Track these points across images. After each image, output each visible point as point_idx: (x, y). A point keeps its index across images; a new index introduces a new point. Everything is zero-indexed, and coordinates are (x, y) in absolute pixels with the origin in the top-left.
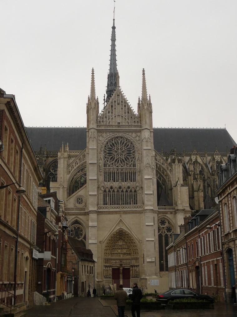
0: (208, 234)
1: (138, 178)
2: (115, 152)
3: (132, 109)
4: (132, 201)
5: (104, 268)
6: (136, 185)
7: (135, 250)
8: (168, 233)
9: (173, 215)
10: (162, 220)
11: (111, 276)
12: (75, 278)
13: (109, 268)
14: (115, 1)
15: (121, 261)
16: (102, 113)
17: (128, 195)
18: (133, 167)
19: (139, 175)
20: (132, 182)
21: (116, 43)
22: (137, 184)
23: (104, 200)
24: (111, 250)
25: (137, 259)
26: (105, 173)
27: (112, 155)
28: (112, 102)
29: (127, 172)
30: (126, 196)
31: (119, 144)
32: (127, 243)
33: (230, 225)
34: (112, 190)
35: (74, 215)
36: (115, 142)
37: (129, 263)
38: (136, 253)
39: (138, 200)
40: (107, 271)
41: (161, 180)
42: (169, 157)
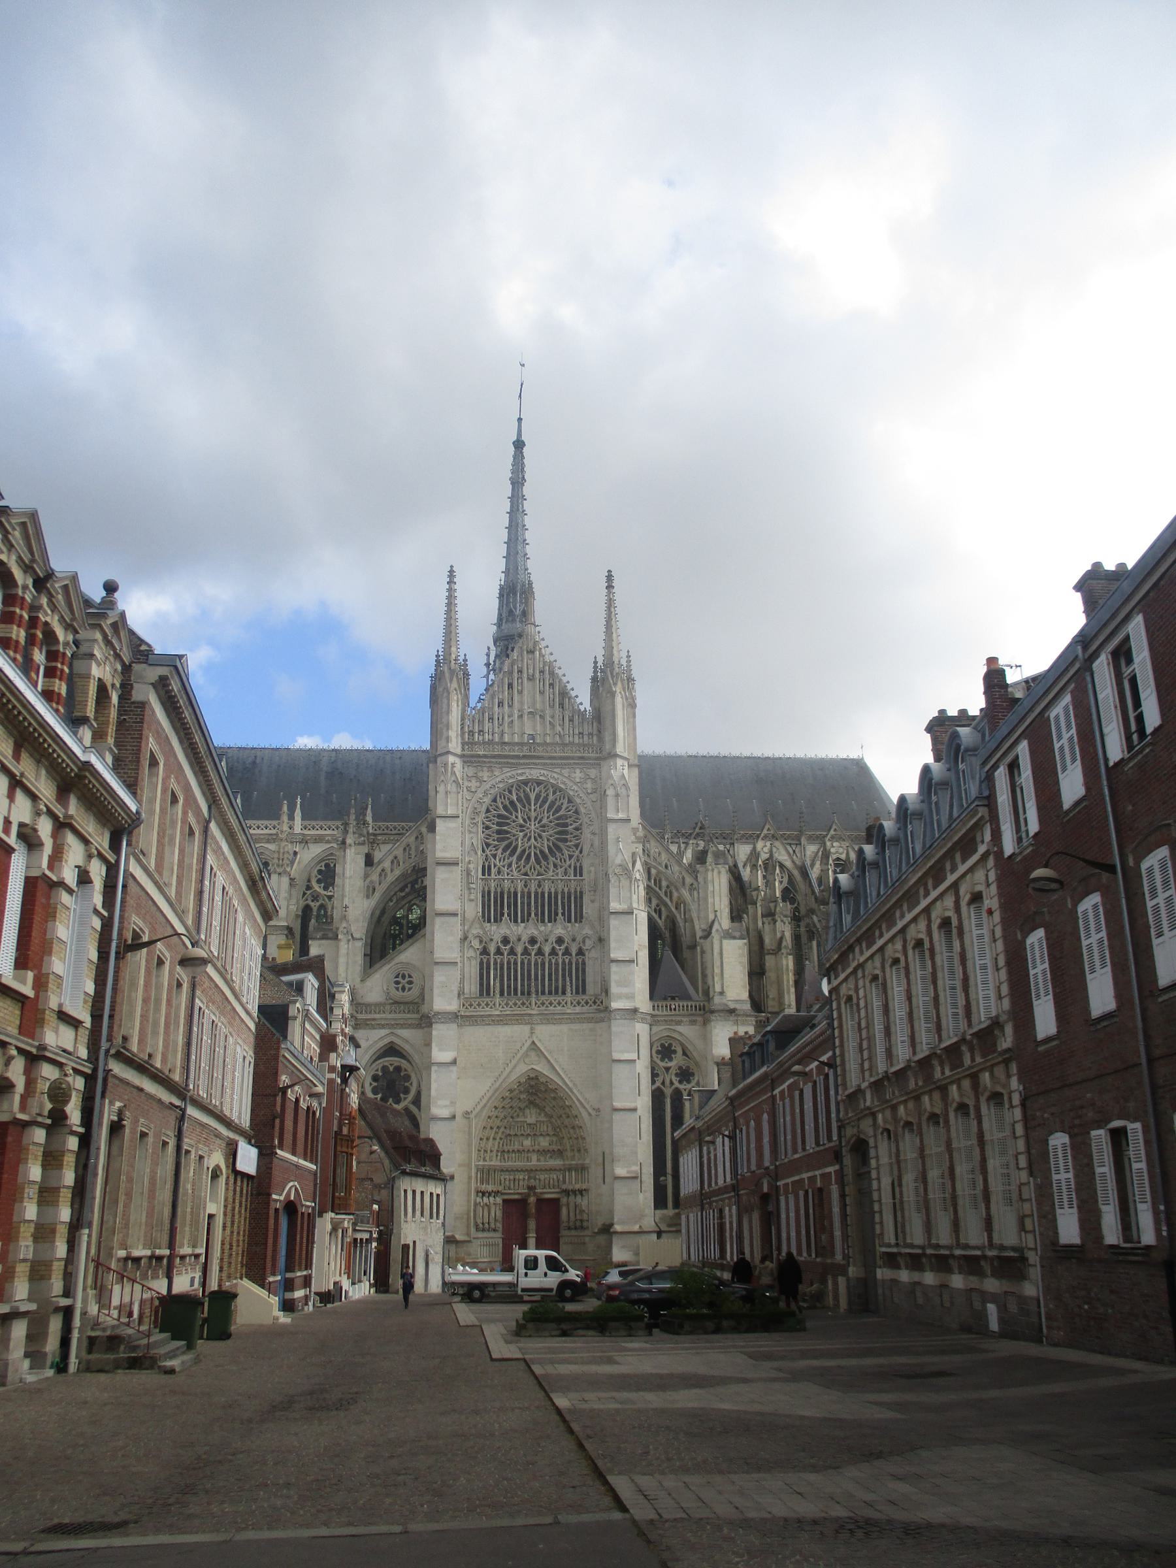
0: (797, 1093)
1: (589, 909)
2: (518, 828)
3: (573, 694)
4: (571, 980)
5: (479, 1200)
6: (584, 932)
7: (577, 1139)
8: (681, 1087)
9: (697, 1027)
10: (662, 1045)
11: (499, 1226)
12: (381, 1231)
13: (492, 1199)
14: (523, 365)
15: (532, 1175)
16: (479, 705)
17: (557, 964)
18: (575, 876)
19: (593, 901)
20: (569, 921)
21: (527, 490)
22: (587, 931)
23: (481, 978)
24: (501, 1139)
25: (583, 1169)
26: (486, 895)
27: (508, 838)
28: (511, 673)
29: (556, 893)
30: (550, 969)
31: (530, 805)
32: (552, 1117)
33: (862, 1065)
34: (505, 949)
35: (383, 1027)
36: (519, 799)
37: (556, 1183)
38: (579, 1151)
39: (589, 980)
40: (486, 1208)
41: (663, 918)
42: (687, 844)
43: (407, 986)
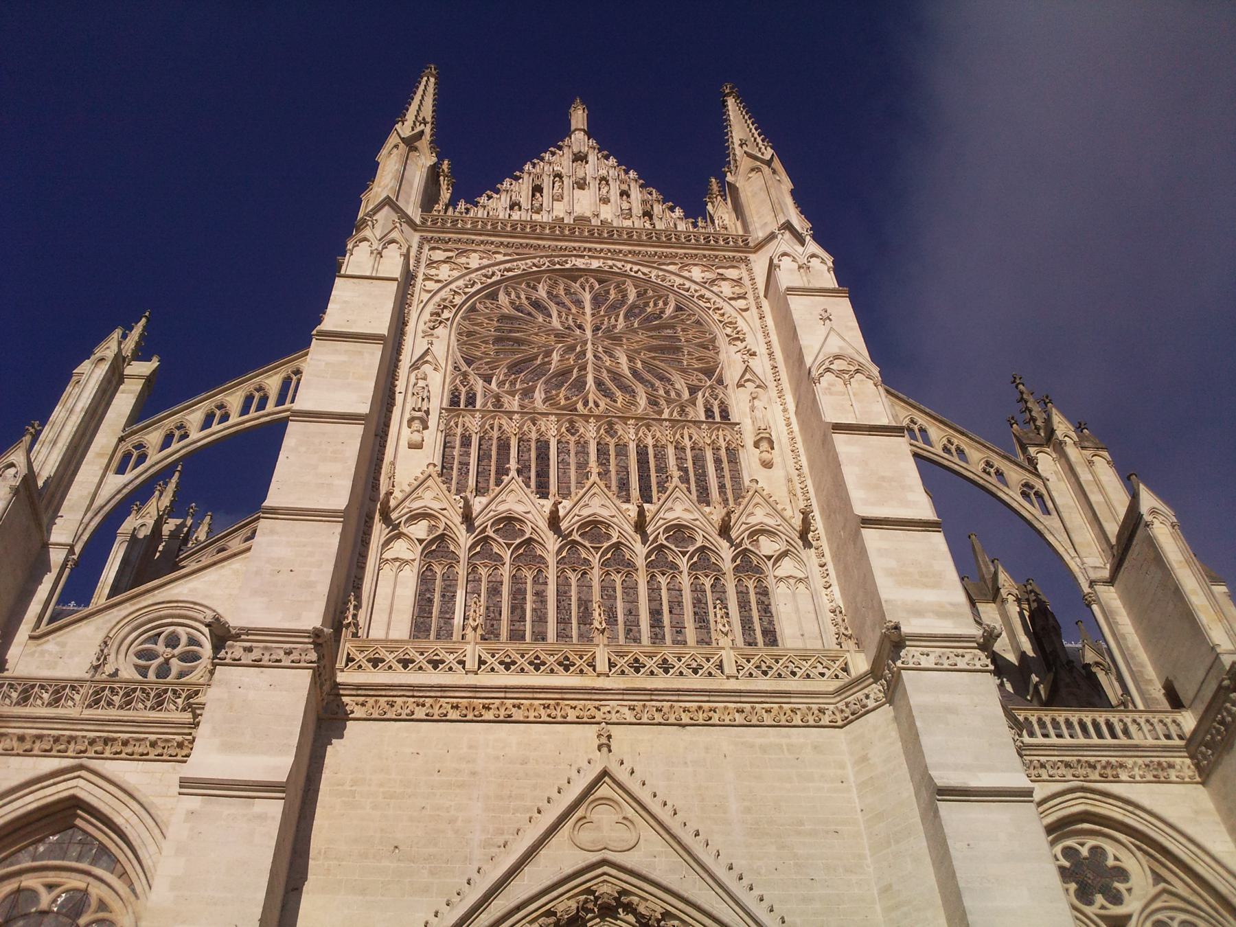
17: (676, 591)
19: (767, 465)
22: (759, 516)
43: (176, 665)
